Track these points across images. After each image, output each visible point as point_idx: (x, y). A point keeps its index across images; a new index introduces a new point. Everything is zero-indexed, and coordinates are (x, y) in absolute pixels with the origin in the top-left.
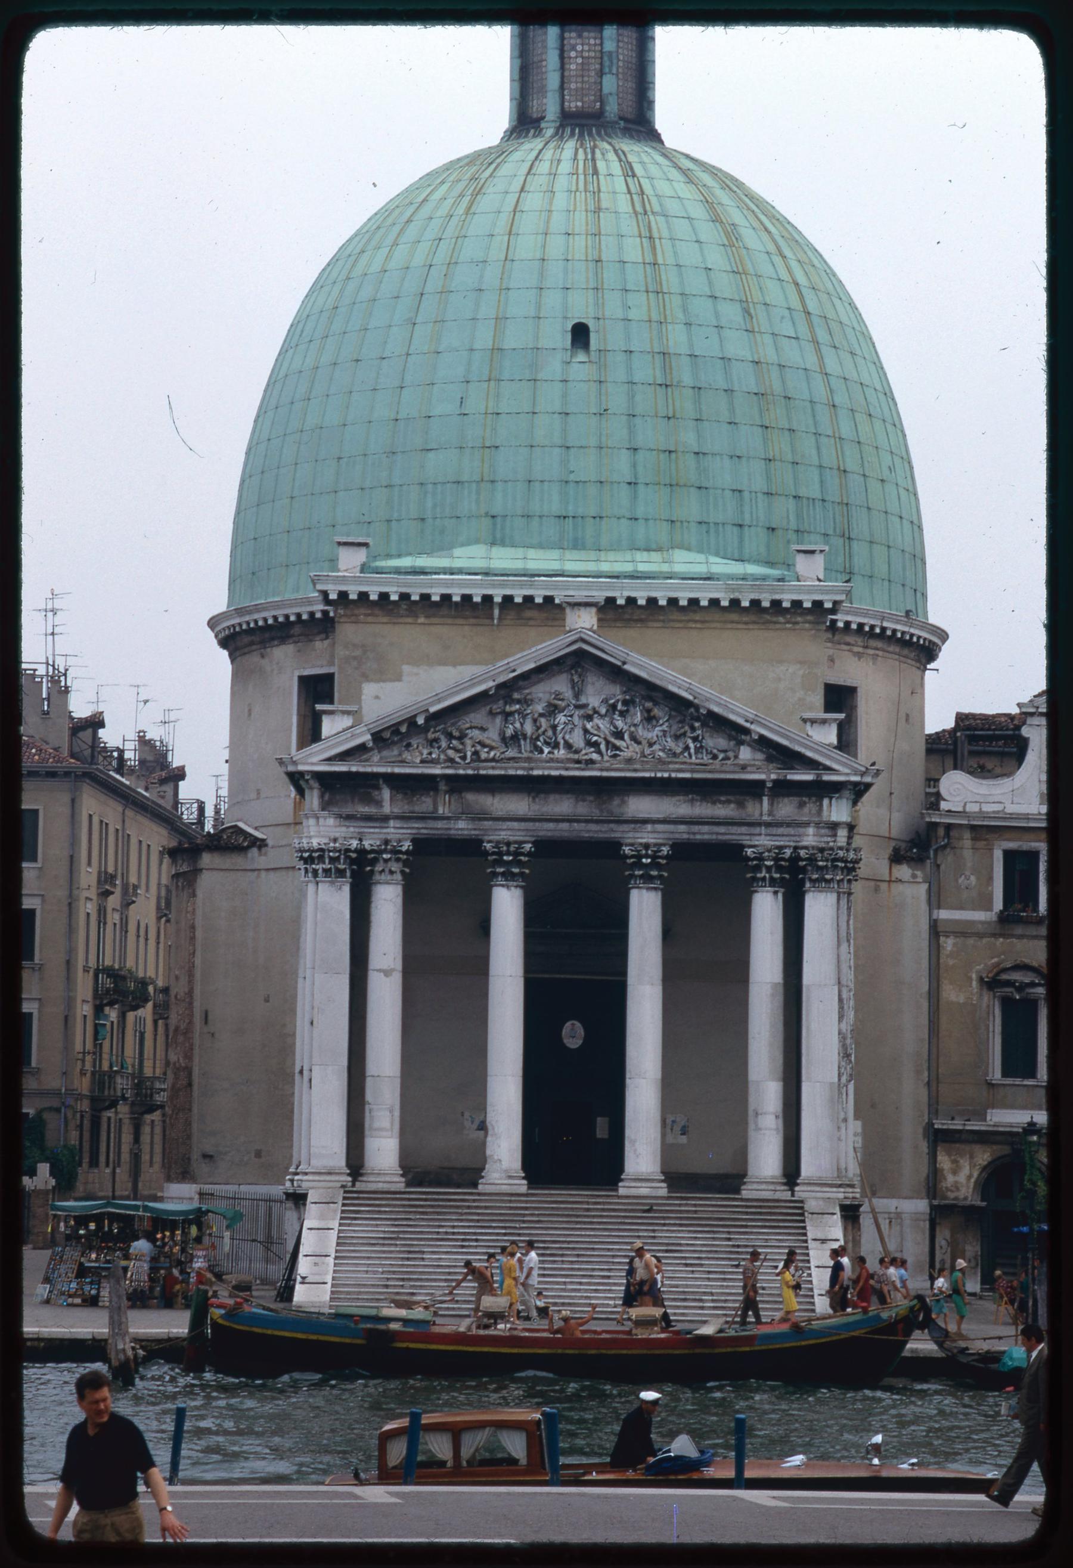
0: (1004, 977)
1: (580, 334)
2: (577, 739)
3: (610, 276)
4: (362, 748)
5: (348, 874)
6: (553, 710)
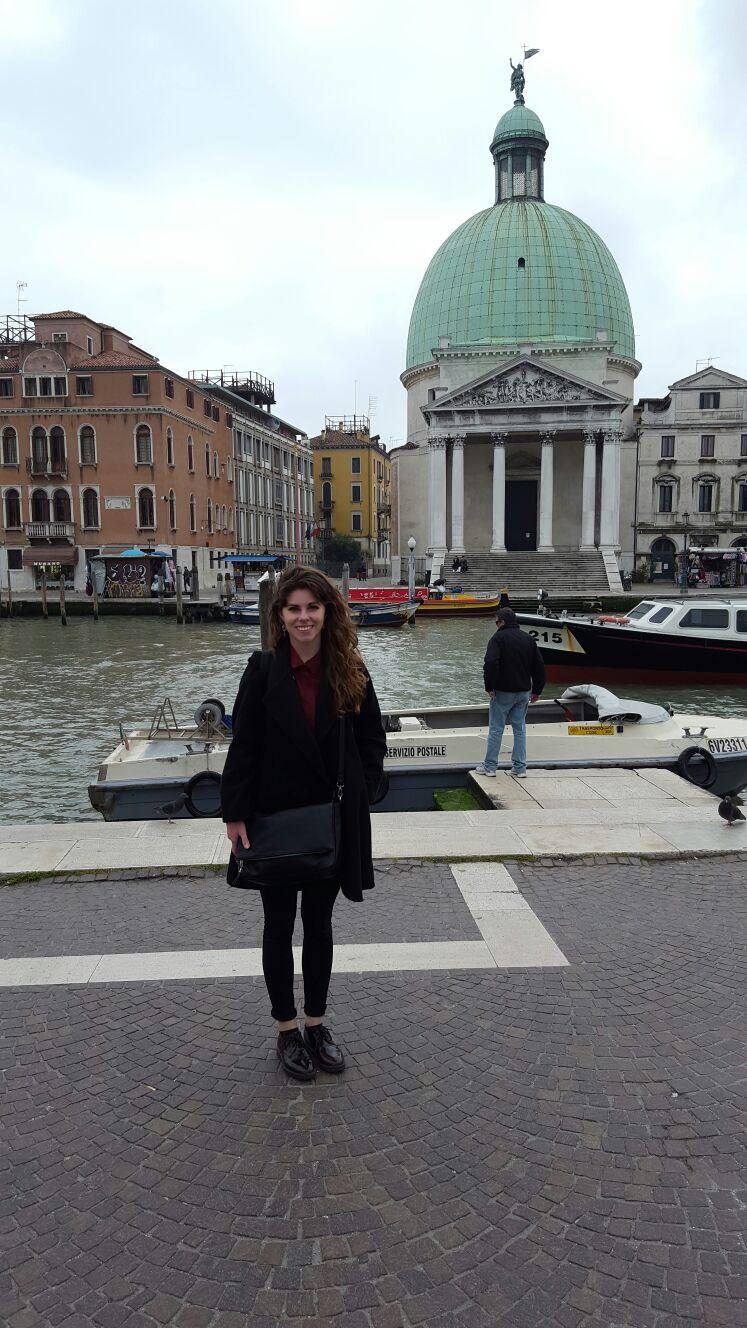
1: (521, 262)
2: (524, 395)
3: (531, 241)
4: (449, 401)
6: (515, 384)
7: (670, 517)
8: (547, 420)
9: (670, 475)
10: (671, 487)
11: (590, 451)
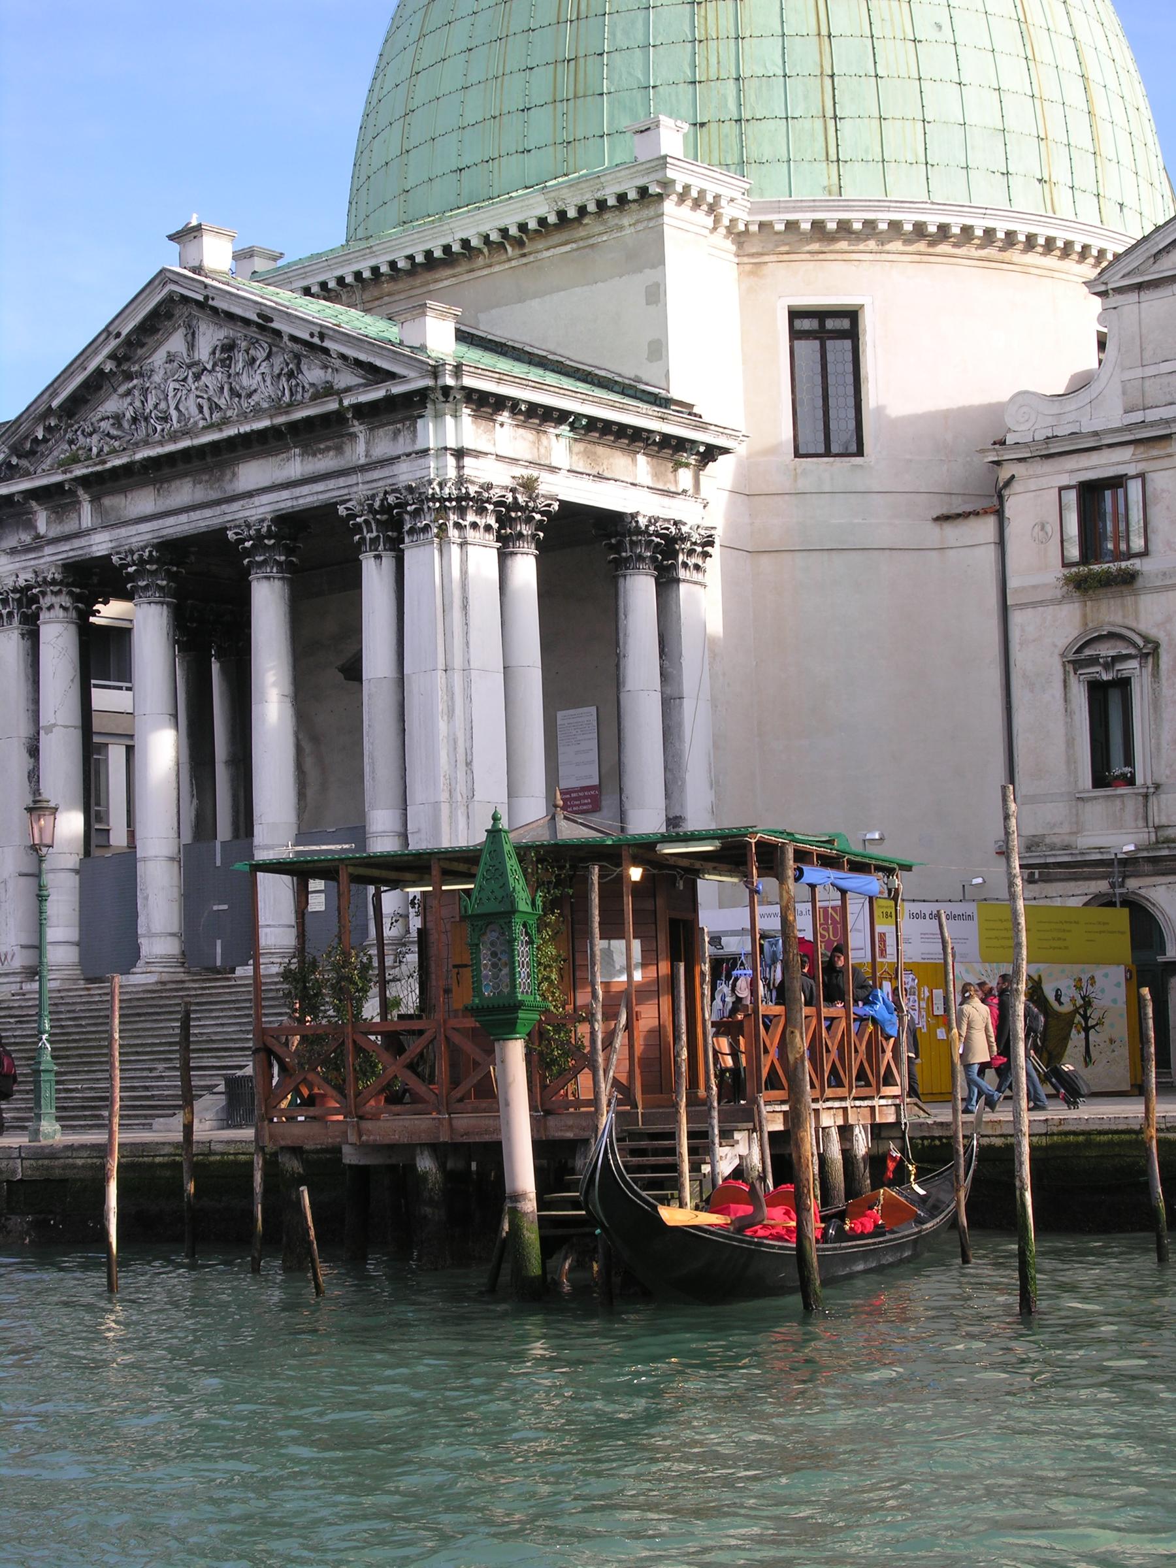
0: (1088, 652)
2: (190, 407)
5: (16, 619)
7: (1132, 806)
8: (251, 486)
9: (1112, 636)
10: (1124, 684)
11: (375, 576)
